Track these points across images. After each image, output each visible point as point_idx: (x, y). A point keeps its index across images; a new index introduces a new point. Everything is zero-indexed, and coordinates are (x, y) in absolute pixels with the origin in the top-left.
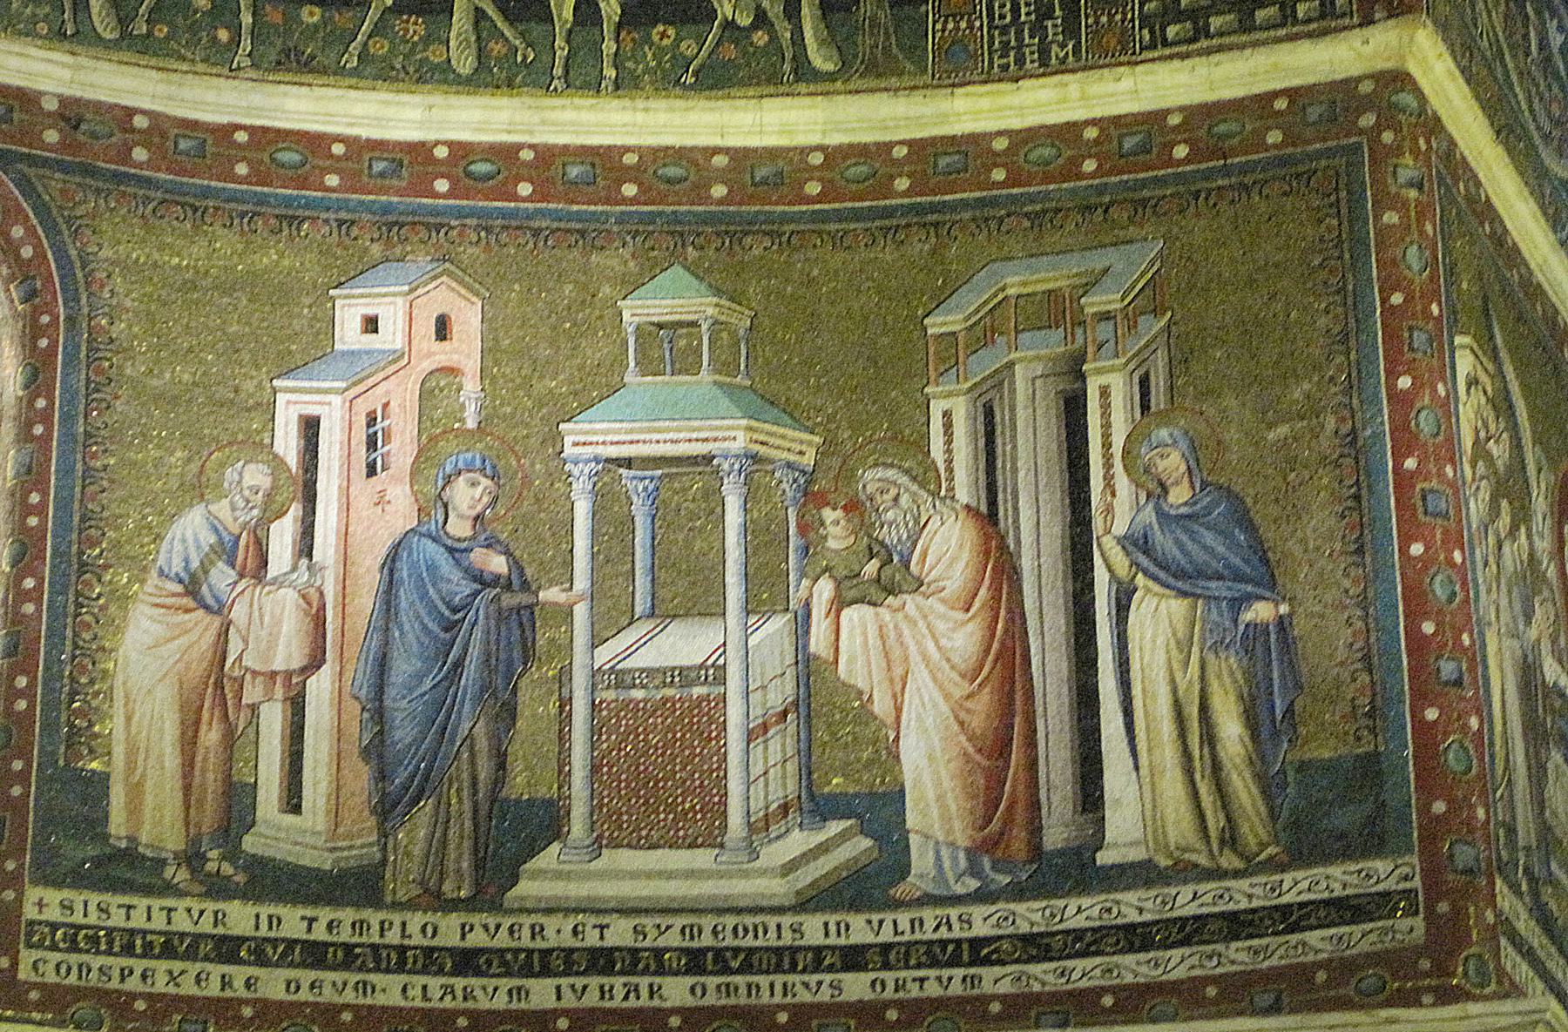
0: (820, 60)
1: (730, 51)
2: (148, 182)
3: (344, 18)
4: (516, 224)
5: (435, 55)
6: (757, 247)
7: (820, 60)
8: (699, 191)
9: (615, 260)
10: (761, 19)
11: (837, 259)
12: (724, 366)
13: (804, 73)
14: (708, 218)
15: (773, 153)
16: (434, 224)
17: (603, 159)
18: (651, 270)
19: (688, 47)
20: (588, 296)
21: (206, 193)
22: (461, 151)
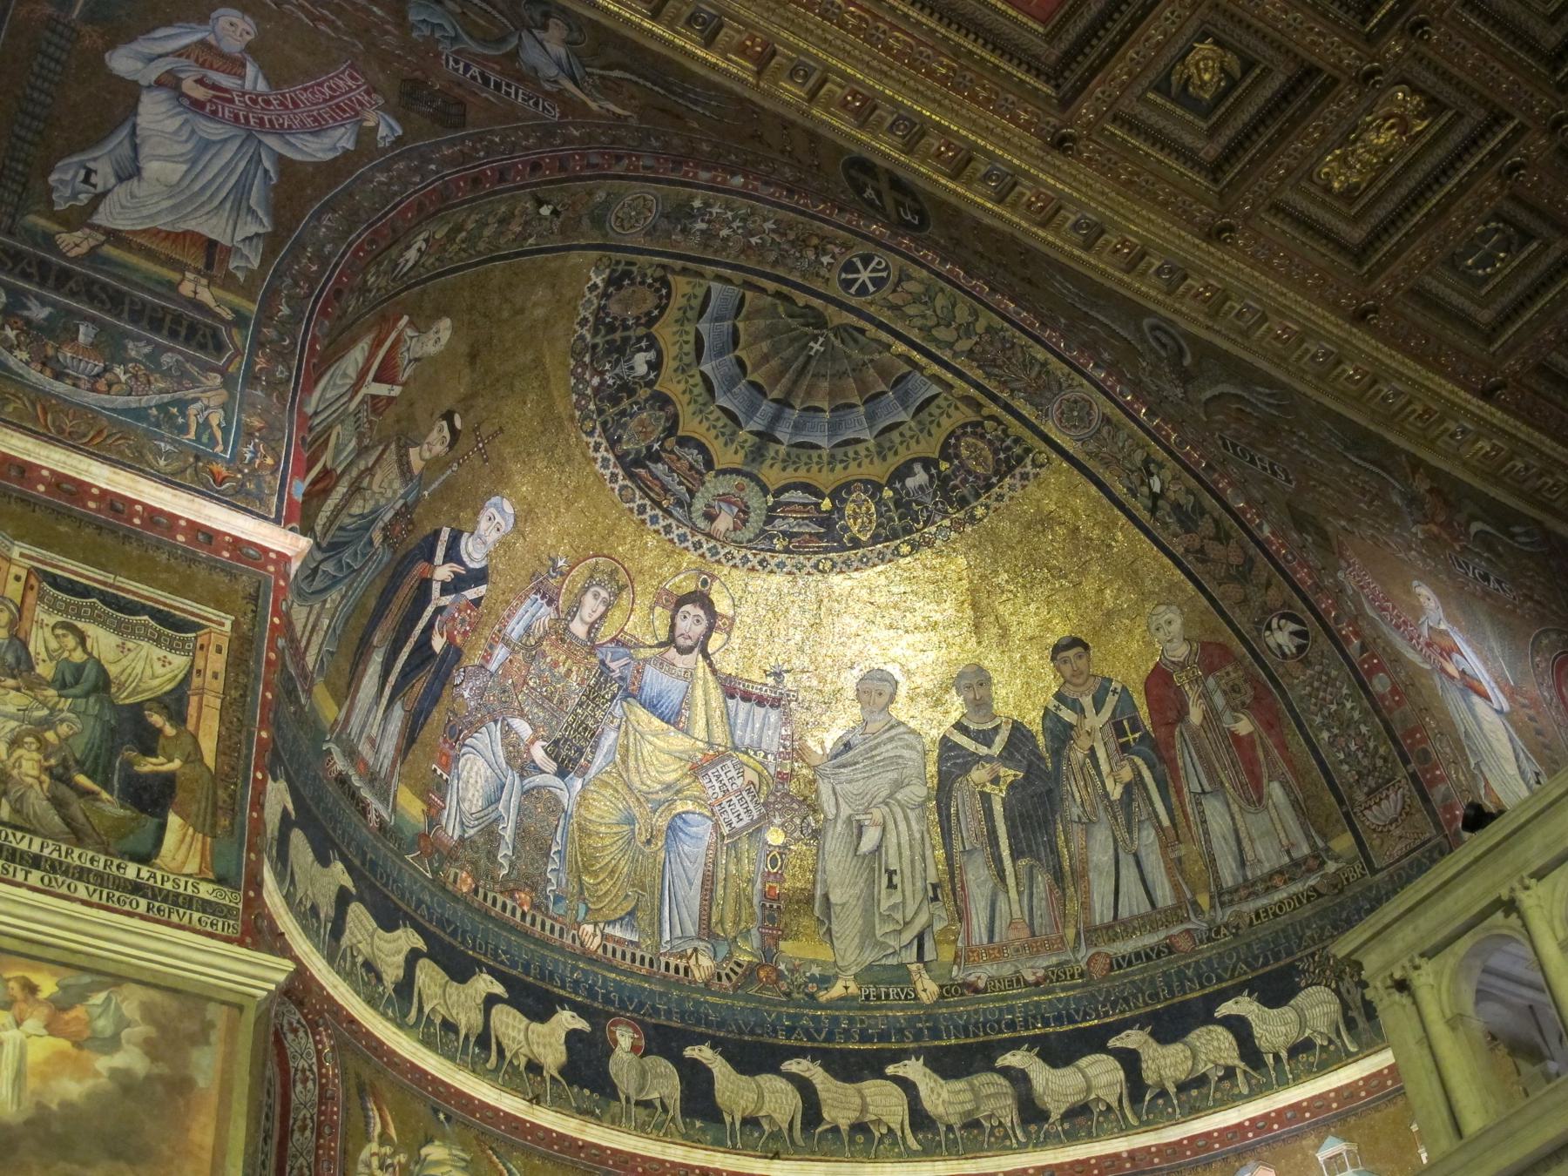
0: (1353, 1049)
1: (1324, 1056)
2: (1161, 1169)
3: (1204, 1091)
4: (1275, 1139)
5: (1236, 1091)
6: (1352, 1120)
7: (1353, 1049)
8: (1329, 1109)
9: (1310, 1141)
10: (1331, 1042)
11: (1377, 1116)
12: (1354, 1165)
13: (1349, 1054)
14: (1335, 1116)
15: (1348, 1086)
16: (1251, 1149)
17: (1296, 1107)
18: (1322, 1140)
19: (1311, 1059)
20: (1306, 1156)
21: (1180, 1165)
22: (1253, 1120)
